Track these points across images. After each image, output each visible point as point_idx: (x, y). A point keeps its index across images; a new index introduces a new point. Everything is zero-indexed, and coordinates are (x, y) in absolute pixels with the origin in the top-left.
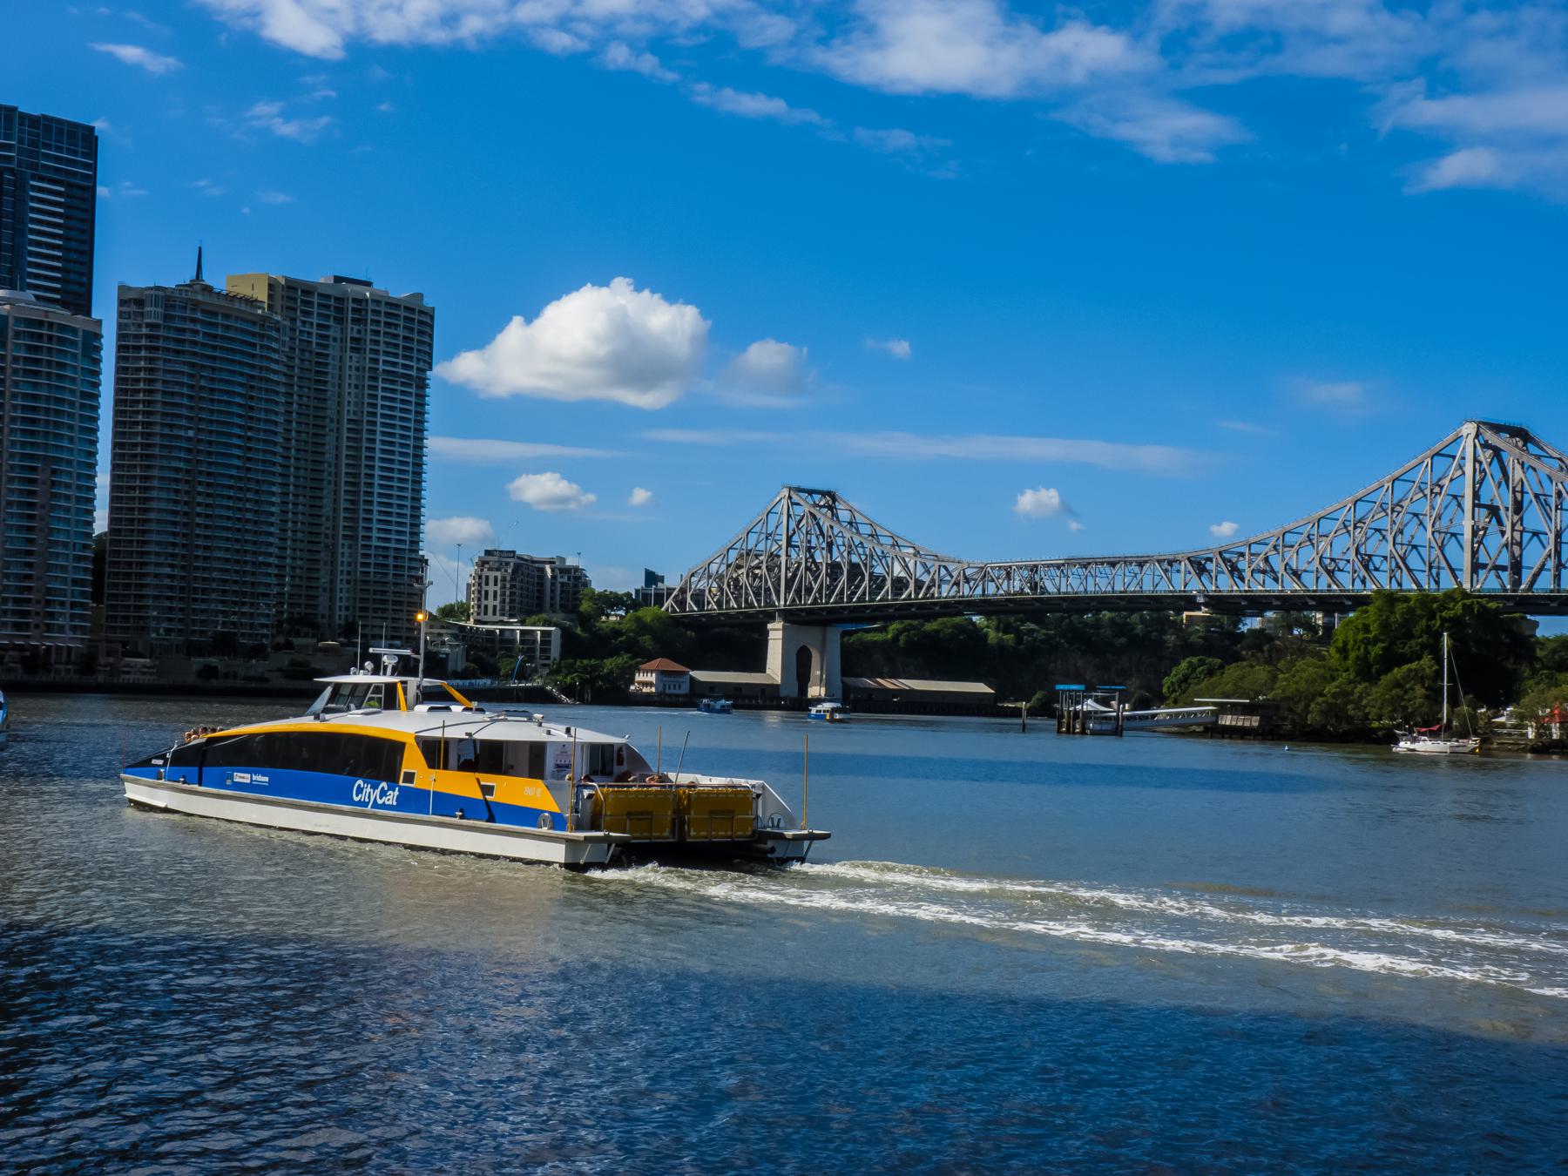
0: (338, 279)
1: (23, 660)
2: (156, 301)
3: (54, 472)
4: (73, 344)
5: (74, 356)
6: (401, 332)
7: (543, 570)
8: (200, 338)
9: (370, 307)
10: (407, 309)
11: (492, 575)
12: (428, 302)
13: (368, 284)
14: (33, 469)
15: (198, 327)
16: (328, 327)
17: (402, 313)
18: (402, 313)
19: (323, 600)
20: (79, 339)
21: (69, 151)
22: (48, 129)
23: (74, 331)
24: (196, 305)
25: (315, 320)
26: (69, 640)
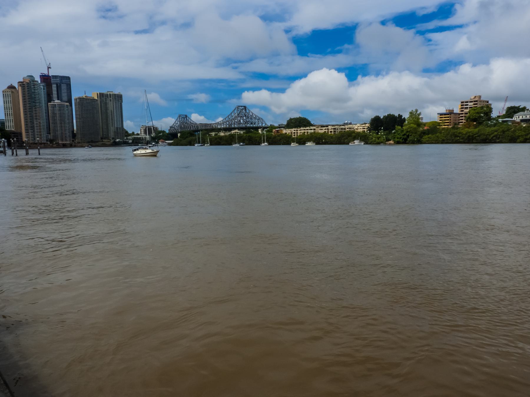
0: (108, 92)
1: (63, 145)
2: (78, 99)
3: (65, 122)
4: (65, 107)
5: (65, 108)
6: (117, 98)
7: (151, 128)
8: (85, 103)
9: (112, 95)
10: (117, 95)
11: (142, 129)
12: (121, 93)
13: (112, 92)
14: (61, 122)
15: (85, 101)
16: (106, 98)
17: (117, 96)
18: (117, 96)
19: (110, 135)
20: (66, 106)
21: (66, 80)
22: (63, 77)
23: (65, 105)
24: (84, 99)
25: (104, 98)
26: (68, 142)
